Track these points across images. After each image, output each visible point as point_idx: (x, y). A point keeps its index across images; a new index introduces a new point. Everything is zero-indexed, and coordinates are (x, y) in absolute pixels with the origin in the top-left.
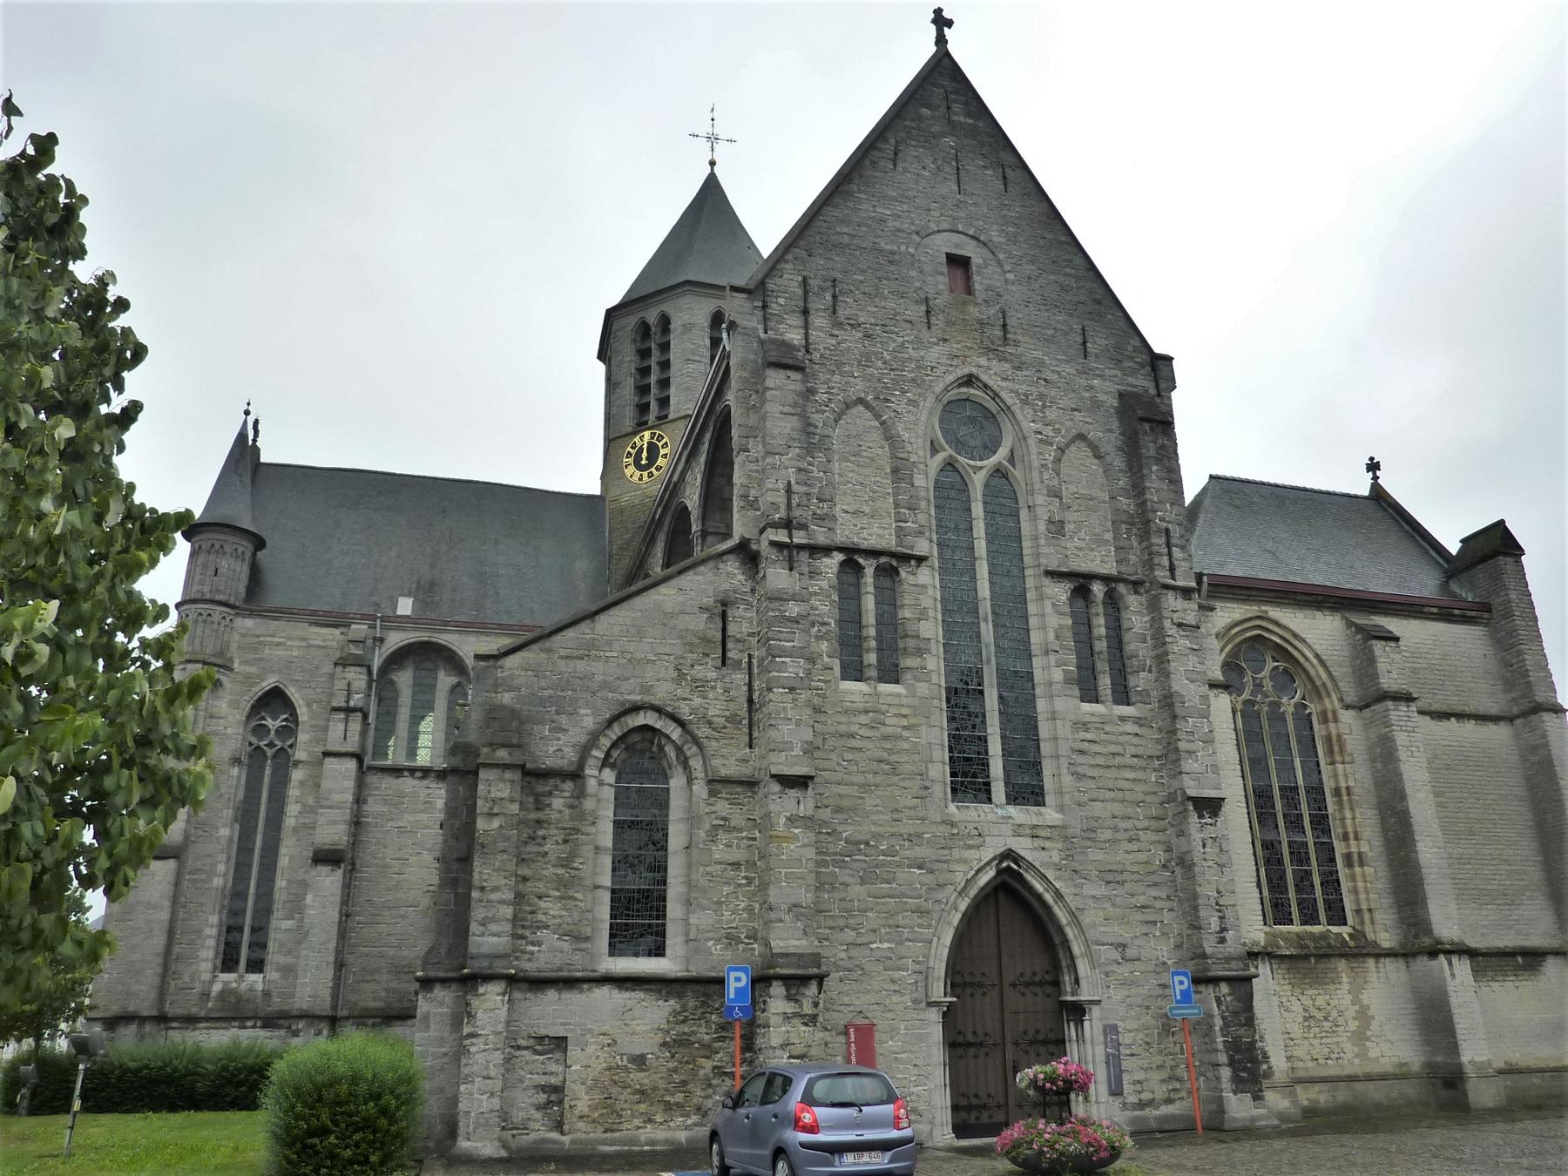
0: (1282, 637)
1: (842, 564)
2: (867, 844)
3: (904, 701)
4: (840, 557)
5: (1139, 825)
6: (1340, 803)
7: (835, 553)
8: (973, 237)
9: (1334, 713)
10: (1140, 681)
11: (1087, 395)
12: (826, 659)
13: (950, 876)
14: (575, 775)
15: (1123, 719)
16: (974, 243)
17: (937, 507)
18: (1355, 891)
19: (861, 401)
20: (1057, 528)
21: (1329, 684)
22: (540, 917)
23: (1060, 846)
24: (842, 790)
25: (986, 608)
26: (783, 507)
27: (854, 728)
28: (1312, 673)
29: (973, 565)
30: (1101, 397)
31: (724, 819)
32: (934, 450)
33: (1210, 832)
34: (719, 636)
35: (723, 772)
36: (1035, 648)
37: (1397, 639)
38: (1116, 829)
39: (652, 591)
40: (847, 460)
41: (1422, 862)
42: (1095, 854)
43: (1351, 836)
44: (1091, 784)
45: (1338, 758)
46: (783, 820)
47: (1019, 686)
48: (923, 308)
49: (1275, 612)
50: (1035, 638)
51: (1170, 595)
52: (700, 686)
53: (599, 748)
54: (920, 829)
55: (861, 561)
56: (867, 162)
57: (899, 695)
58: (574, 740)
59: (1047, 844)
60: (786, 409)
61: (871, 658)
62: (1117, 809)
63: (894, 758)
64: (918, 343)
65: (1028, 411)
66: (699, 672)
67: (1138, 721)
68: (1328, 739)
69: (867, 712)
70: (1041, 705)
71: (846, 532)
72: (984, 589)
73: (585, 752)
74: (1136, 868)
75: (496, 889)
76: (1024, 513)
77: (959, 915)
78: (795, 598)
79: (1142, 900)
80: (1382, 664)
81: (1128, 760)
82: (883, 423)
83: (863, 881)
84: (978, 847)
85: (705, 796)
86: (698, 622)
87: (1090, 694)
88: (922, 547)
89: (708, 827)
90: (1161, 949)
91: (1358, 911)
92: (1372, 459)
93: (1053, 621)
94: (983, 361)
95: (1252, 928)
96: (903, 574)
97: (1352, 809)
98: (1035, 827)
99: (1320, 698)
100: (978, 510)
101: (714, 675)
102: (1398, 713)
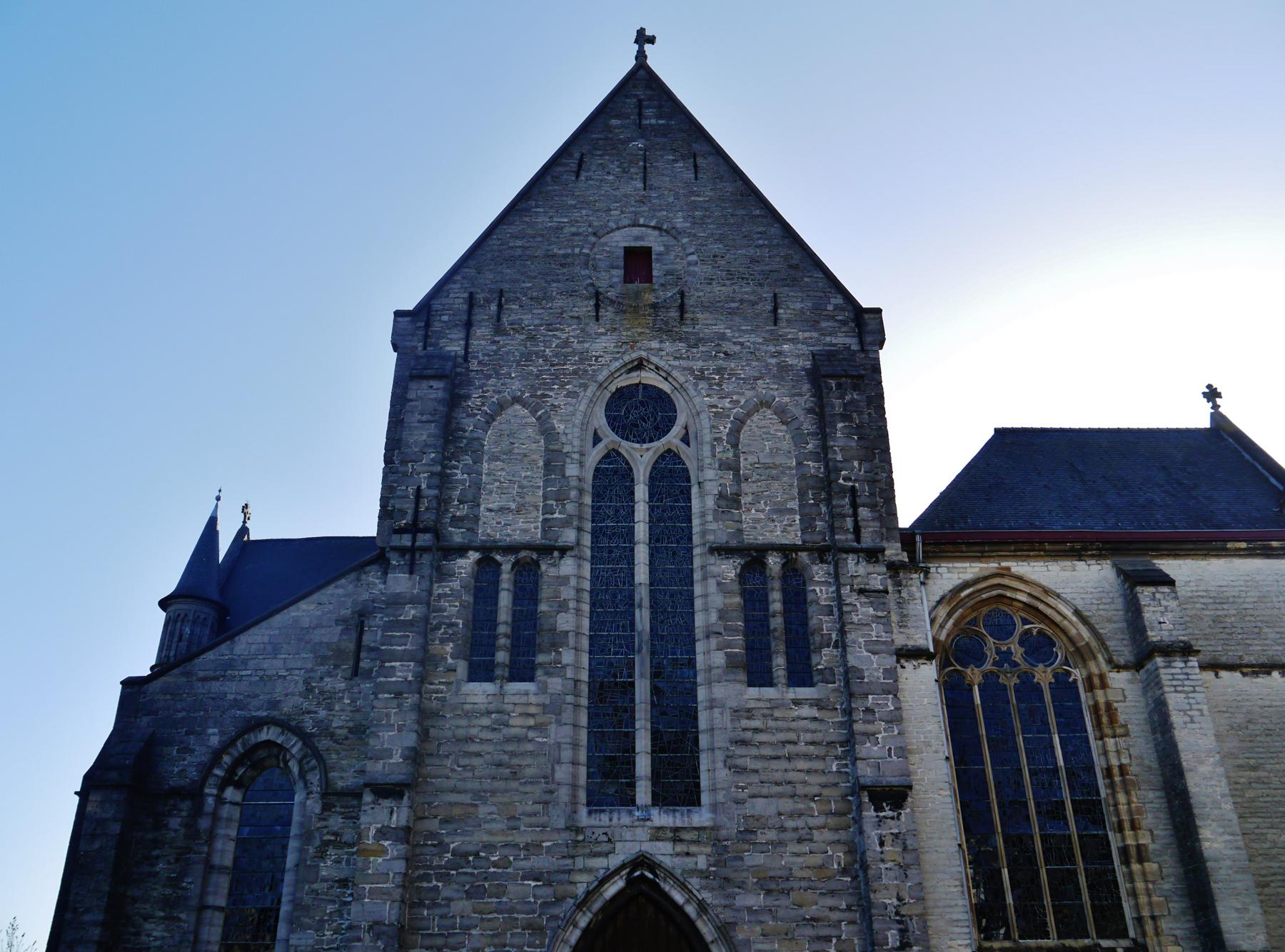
0: (1030, 595)
1: (479, 562)
2: (477, 855)
3: (533, 699)
4: (474, 556)
5: (812, 822)
6: (1112, 786)
7: (471, 553)
8: (654, 228)
9: (1102, 677)
10: (825, 658)
11: (773, 361)
12: (450, 661)
13: (570, 888)
14: (194, 793)
15: (797, 702)
16: (656, 233)
17: (597, 496)
18: (1133, 894)
19: (516, 400)
20: (729, 501)
21: (1094, 644)
22: (144, 938)
23: (708, 850)
24: (453, 798)
25: (642, 594)
26: (410, 512)
27: (474, 731)
28: (1073, 632)
29: (632, 550)
30: (790, 361)
31: (336, 834)
32: (597, 440)
33: (892, 827)
34: (352, 646)
35: (340, 784)
36: (699, 633)
37: (1170, 582)
38: (782, 829)
39: (292, 608)
40: (498, 459)
41: (1206, 854)
42: (755, 859)
43: (1127, 825)
44: (755, 779)
45: (1108, 731)
46: (372, 832)
48: (592, 302)
49: (1018, 567)
50: (699, 620)
51: (851, 560)
52: (328, 699)
53: (220, 767)
54: (539, 838)
55: (498, 558)
56: (549, 179)
57: (527, 694)
58: (198, 760)
59: (693, 849)
60: (424, 418)
61: (502, 657)
62: (787, 805)
63: (515, 761)
64: (585, 336)
65: (703, 385)
66: (328, 683)
67: (818, 704)
68: (1095, 708)
69: (489, 713)
70: (702, 693)
71: (491, 528)
72: (642, 574)
73: (206, 770)
74: (805, 874)
75: (88, 911)
76: (695, 490)
77: (578, 933)
78: (413, 601)
79: (812, 911)
80: (1149, 615)
81: (802, 748)
82: (539, 419)
83: (469, 895)
84: (606, 855)
85: (317, 811)
86: (332, 634)
87: (759, 675)
88: (569, 536)
89: (318, 843)
91: (1139, 920)
92: (1209, 386)
93: (718, 600)
94: (655, 344)
96: (543, 567)
97: (1127, 793)
98: (676, 830)
99: (1084, 661)
100: (641, 492)
101: (343, 685)
102: (1170, 672)
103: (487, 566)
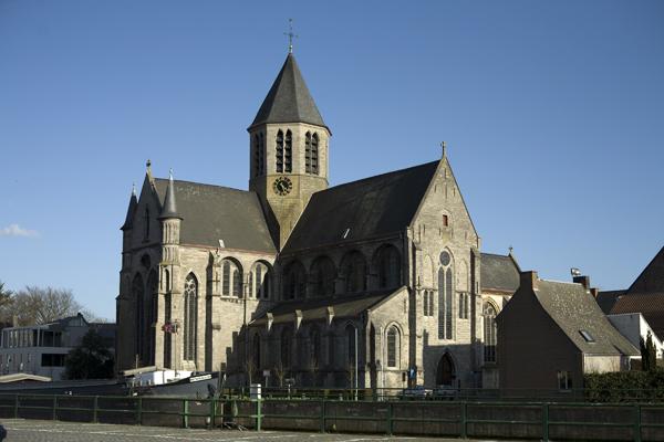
47: (449, 315)
90: (468, 367)
95: (483, 363)
103: (426, 292)
